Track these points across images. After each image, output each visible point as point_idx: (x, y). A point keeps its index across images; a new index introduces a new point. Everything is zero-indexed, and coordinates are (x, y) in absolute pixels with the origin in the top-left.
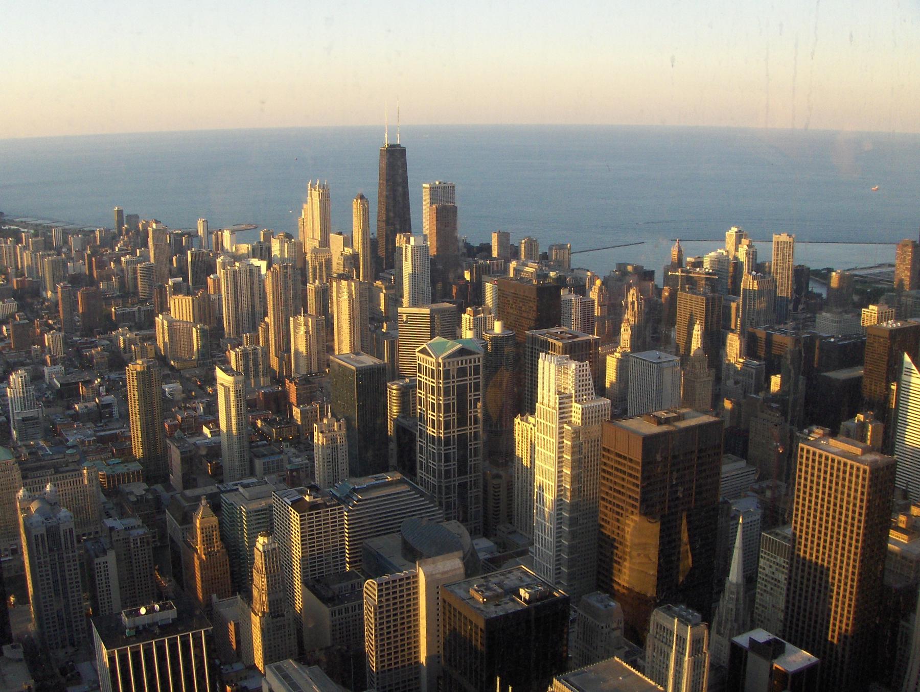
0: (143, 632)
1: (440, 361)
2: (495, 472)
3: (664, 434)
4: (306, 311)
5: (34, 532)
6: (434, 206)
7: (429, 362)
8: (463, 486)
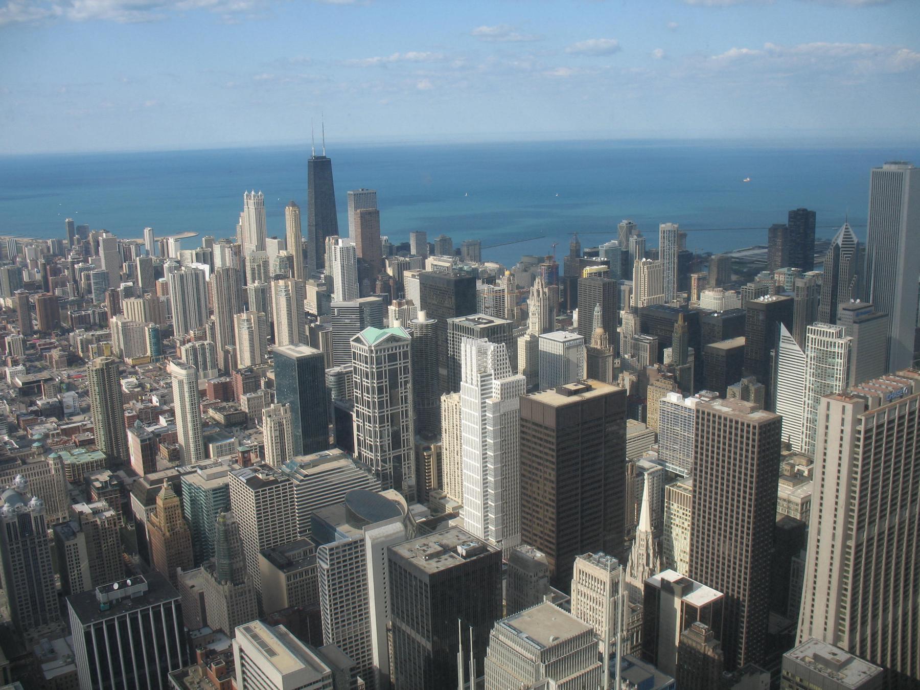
0: (114, 606)
2: (426, 444)
3: (575, 404)
4: (247, 309)
6: (358, 211)
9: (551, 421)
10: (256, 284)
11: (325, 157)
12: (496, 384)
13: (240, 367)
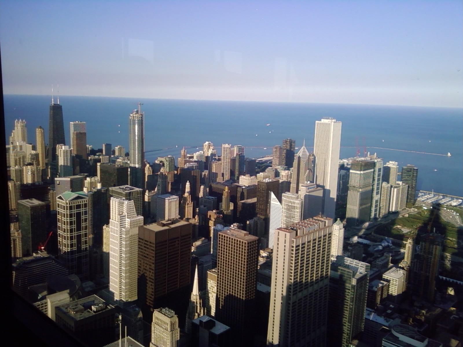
1: (68, 202)
6: (75, 132)
9: (153, 241)
10: (17, 167)
11: (59, 105)
12: (128, 221)
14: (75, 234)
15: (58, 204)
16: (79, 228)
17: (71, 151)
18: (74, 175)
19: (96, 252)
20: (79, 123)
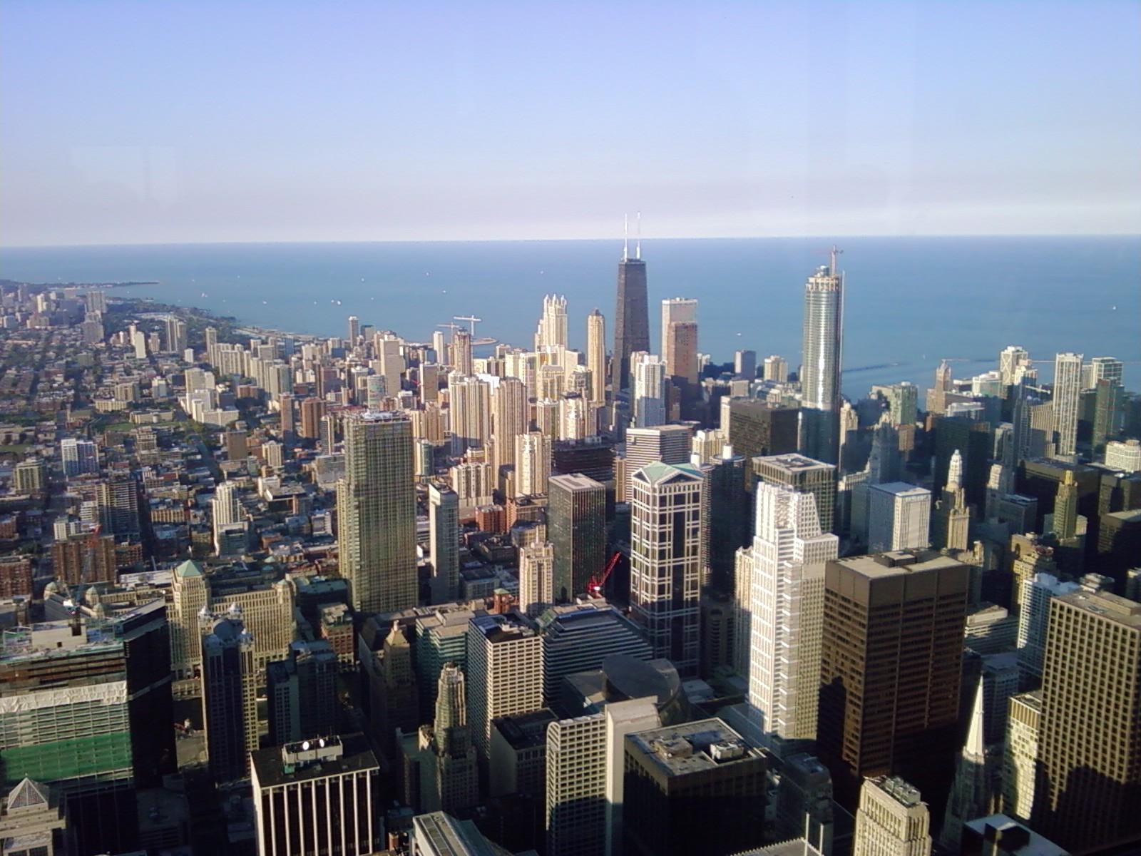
1: (656, 486)
5: (209, 655)
6: (673, 324)
7: (644, 487)
8: (678, 621)
9: (863, 597)
10: (547, 402)
11: (638, 261)
13: (518, 495)
14: (670, 563)
15: (635, 490)
16: (679, 551)
17: (662, 368)
18: (667, 423)
19: (717, 612)
20: (684, 302)
